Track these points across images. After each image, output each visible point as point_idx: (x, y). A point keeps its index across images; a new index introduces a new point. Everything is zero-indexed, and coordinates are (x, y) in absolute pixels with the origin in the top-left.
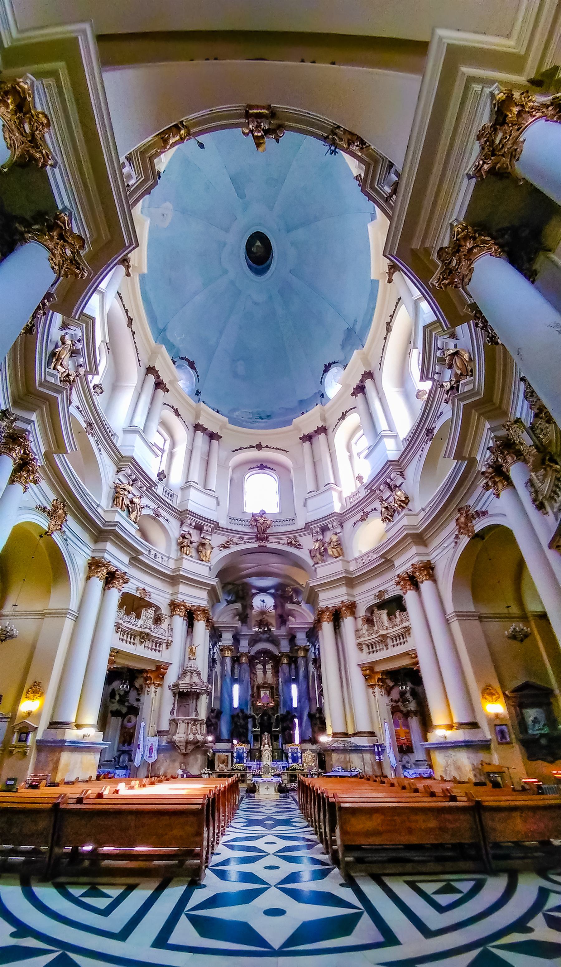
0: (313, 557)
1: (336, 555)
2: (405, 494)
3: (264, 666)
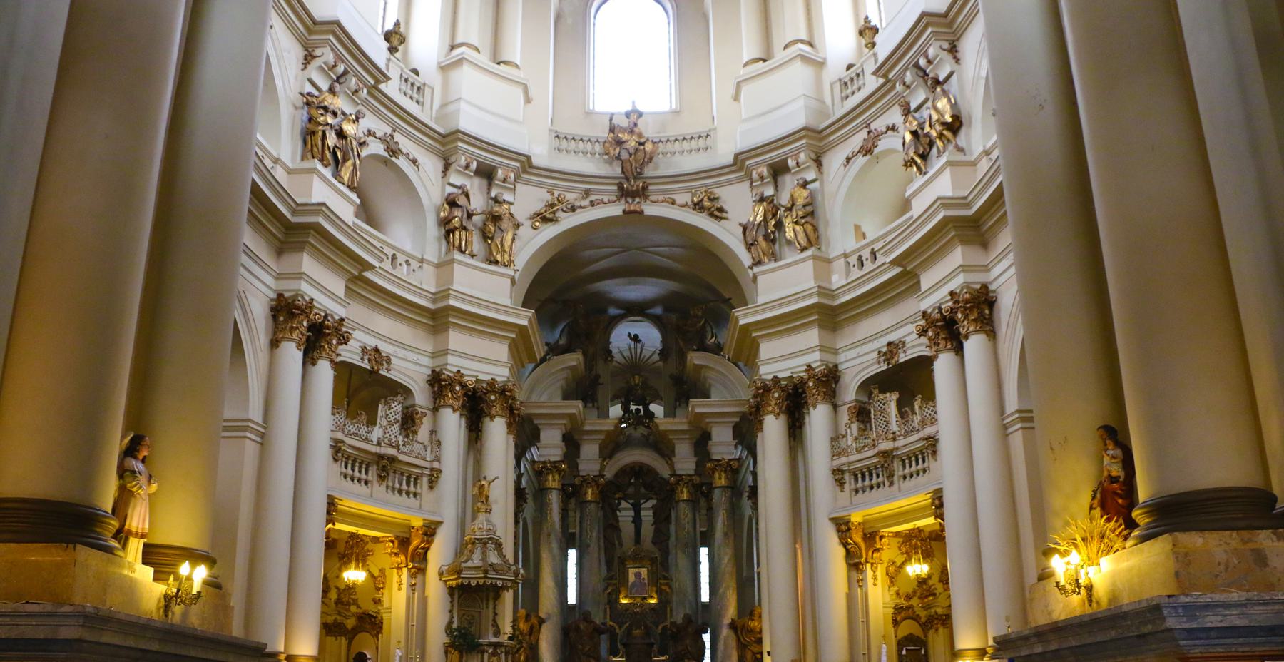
0: (750, 246)
1: (804, 243)
2: (954, 106)
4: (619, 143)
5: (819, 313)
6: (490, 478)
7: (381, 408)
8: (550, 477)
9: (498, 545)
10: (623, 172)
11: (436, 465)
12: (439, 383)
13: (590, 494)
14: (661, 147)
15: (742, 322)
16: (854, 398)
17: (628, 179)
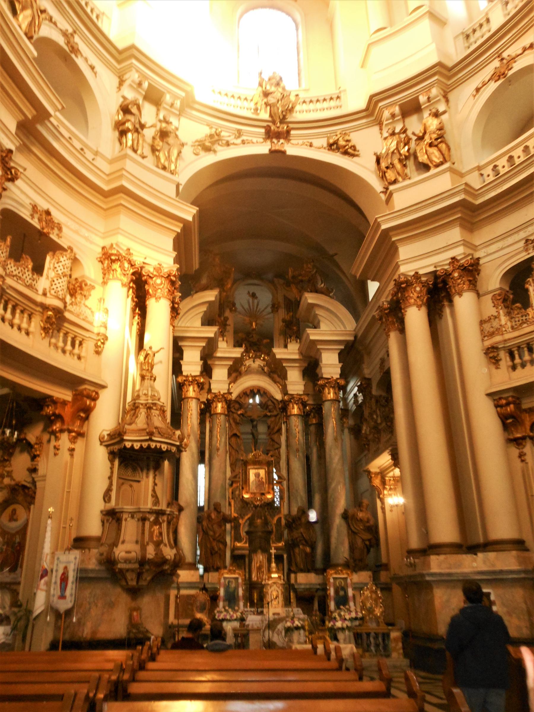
3: (255, 427)
4: (266, 94)
5: (461, 211)
6: (154, 349)
7: (49, 261)
8: (191, 388)
9: (163, 411)
10: (271, 115)
11: (102, 330)
12: (109, 258)
13: (219, 407)
14: (298, 108)
15: (384, 227)
16: (498, 286)
17: (274, 122)
